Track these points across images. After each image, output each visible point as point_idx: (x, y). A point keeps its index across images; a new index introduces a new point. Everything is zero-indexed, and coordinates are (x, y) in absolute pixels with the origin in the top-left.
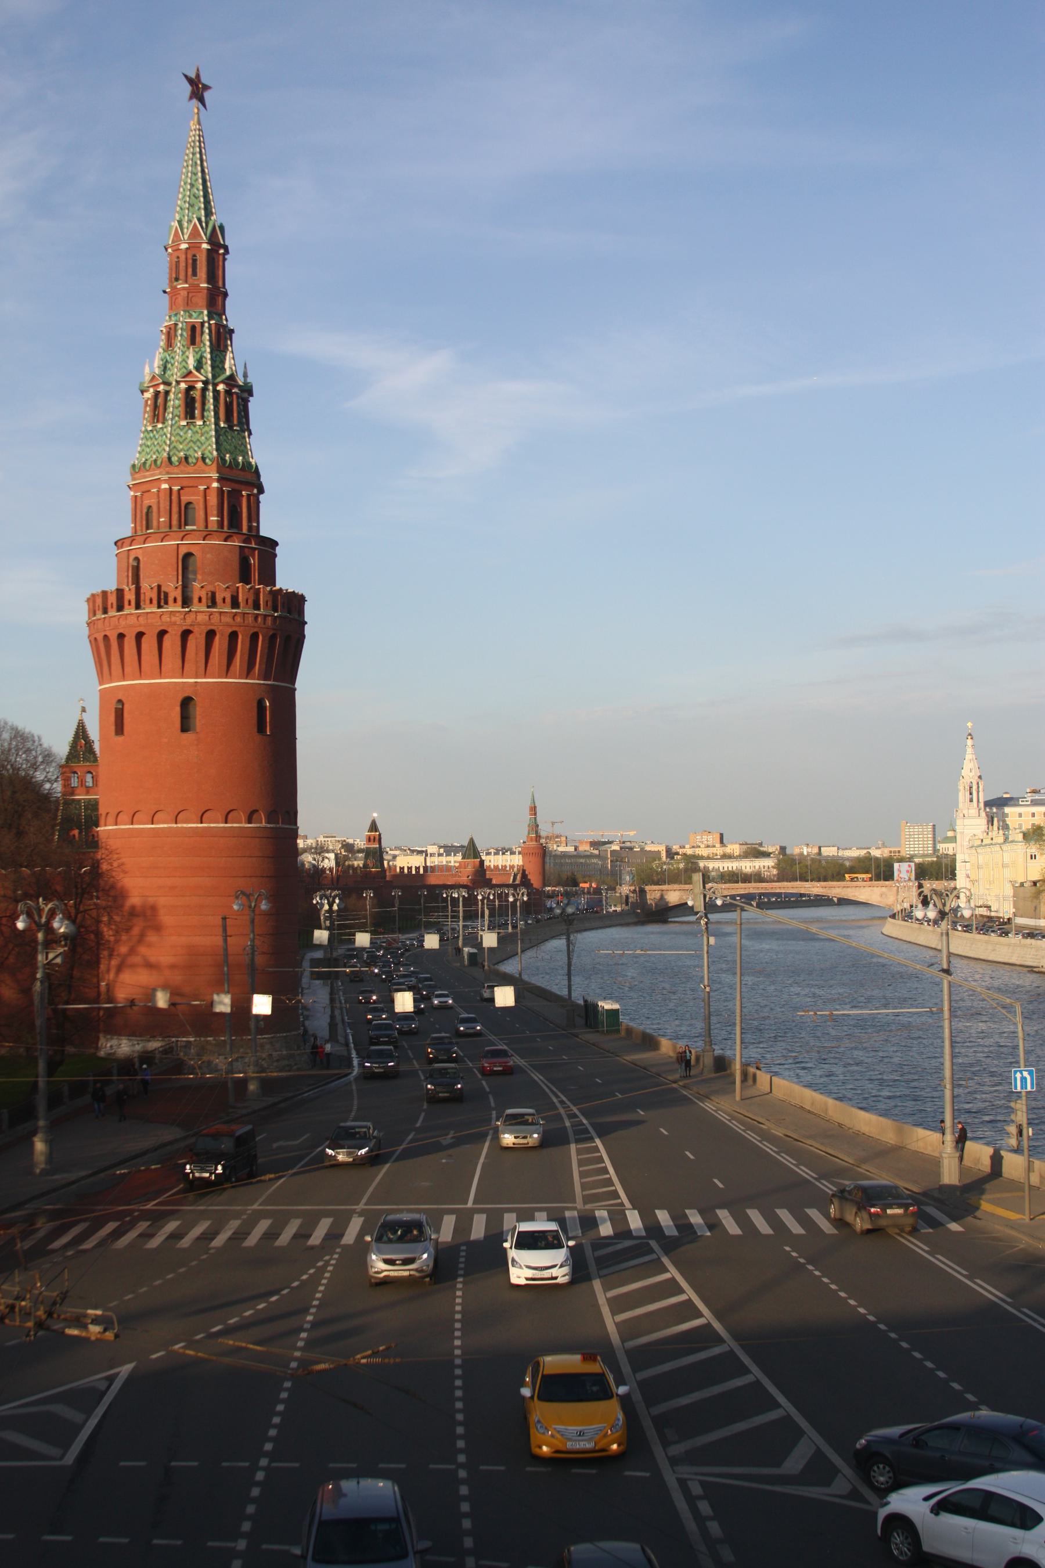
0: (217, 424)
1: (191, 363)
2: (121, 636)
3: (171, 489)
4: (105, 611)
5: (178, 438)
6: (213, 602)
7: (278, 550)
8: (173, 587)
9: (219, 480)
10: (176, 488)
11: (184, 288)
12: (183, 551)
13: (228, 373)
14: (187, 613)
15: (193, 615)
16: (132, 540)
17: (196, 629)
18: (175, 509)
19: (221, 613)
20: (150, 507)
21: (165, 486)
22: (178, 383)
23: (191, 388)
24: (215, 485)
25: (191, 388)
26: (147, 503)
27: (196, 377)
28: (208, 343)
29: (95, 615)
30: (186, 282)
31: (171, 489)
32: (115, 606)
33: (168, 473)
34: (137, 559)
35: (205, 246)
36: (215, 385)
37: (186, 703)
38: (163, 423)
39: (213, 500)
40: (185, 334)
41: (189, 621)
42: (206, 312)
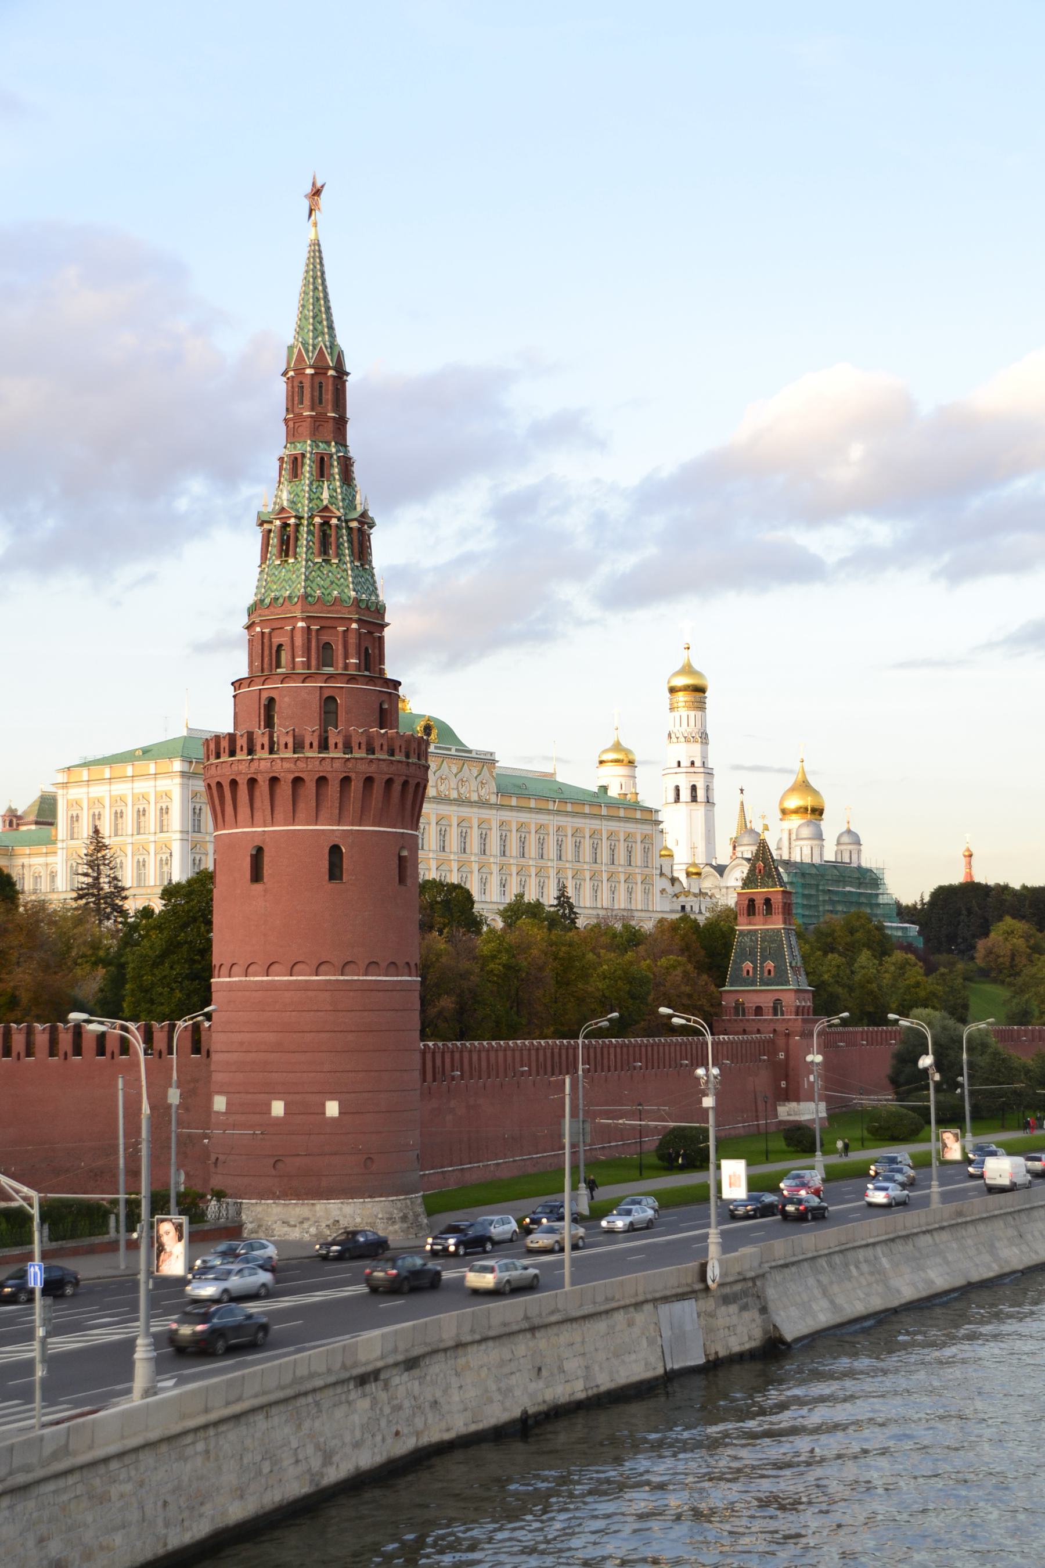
0: (352, 562)
1: (325, 495)
2: (252, 782)
3: (308, 627)
4: (232, 753)
5: (273, 578)
6: (298, 746)
7: (402, 691)
8: (310, 733)
9: (359, 621)
10: (267, 630)
11: (311, 417)
12: (327, 694)
13: (360, 509)
14: (252, 759)
15: (256, 763)
16: (250, 680)
17: (259, 778)
18: (267, 652)
19: (282, 759)
20: (280, 646)
21: (300, 624)
22: (311, 517)
23: (326, 523)
24: (354, 626)
25: (326, 523)
26: (276, 641)
27: (332, 512)
28: (337, 477)
29: (218, 756)
30: (312, 410)
31: (308, 627)
32: (227, 751)
33: (260, 616)
34: (271, 700)
35: (331, 372)
36: (347, 521)
37: (335, 851)
38: (296, 559)
39: (352, 640)
40: (314, 466)
41: (252, 770)
42: (333, 444)
